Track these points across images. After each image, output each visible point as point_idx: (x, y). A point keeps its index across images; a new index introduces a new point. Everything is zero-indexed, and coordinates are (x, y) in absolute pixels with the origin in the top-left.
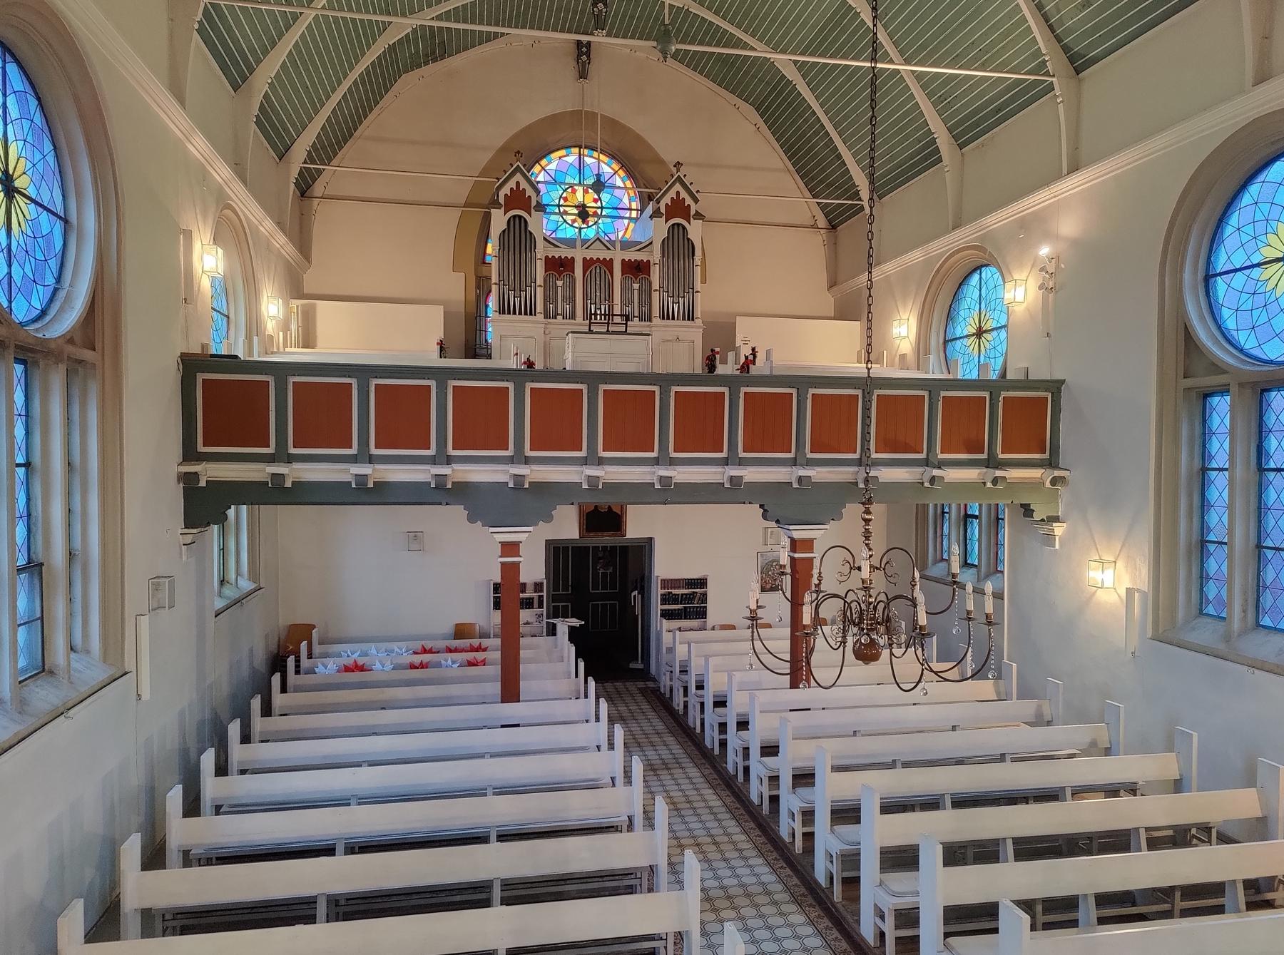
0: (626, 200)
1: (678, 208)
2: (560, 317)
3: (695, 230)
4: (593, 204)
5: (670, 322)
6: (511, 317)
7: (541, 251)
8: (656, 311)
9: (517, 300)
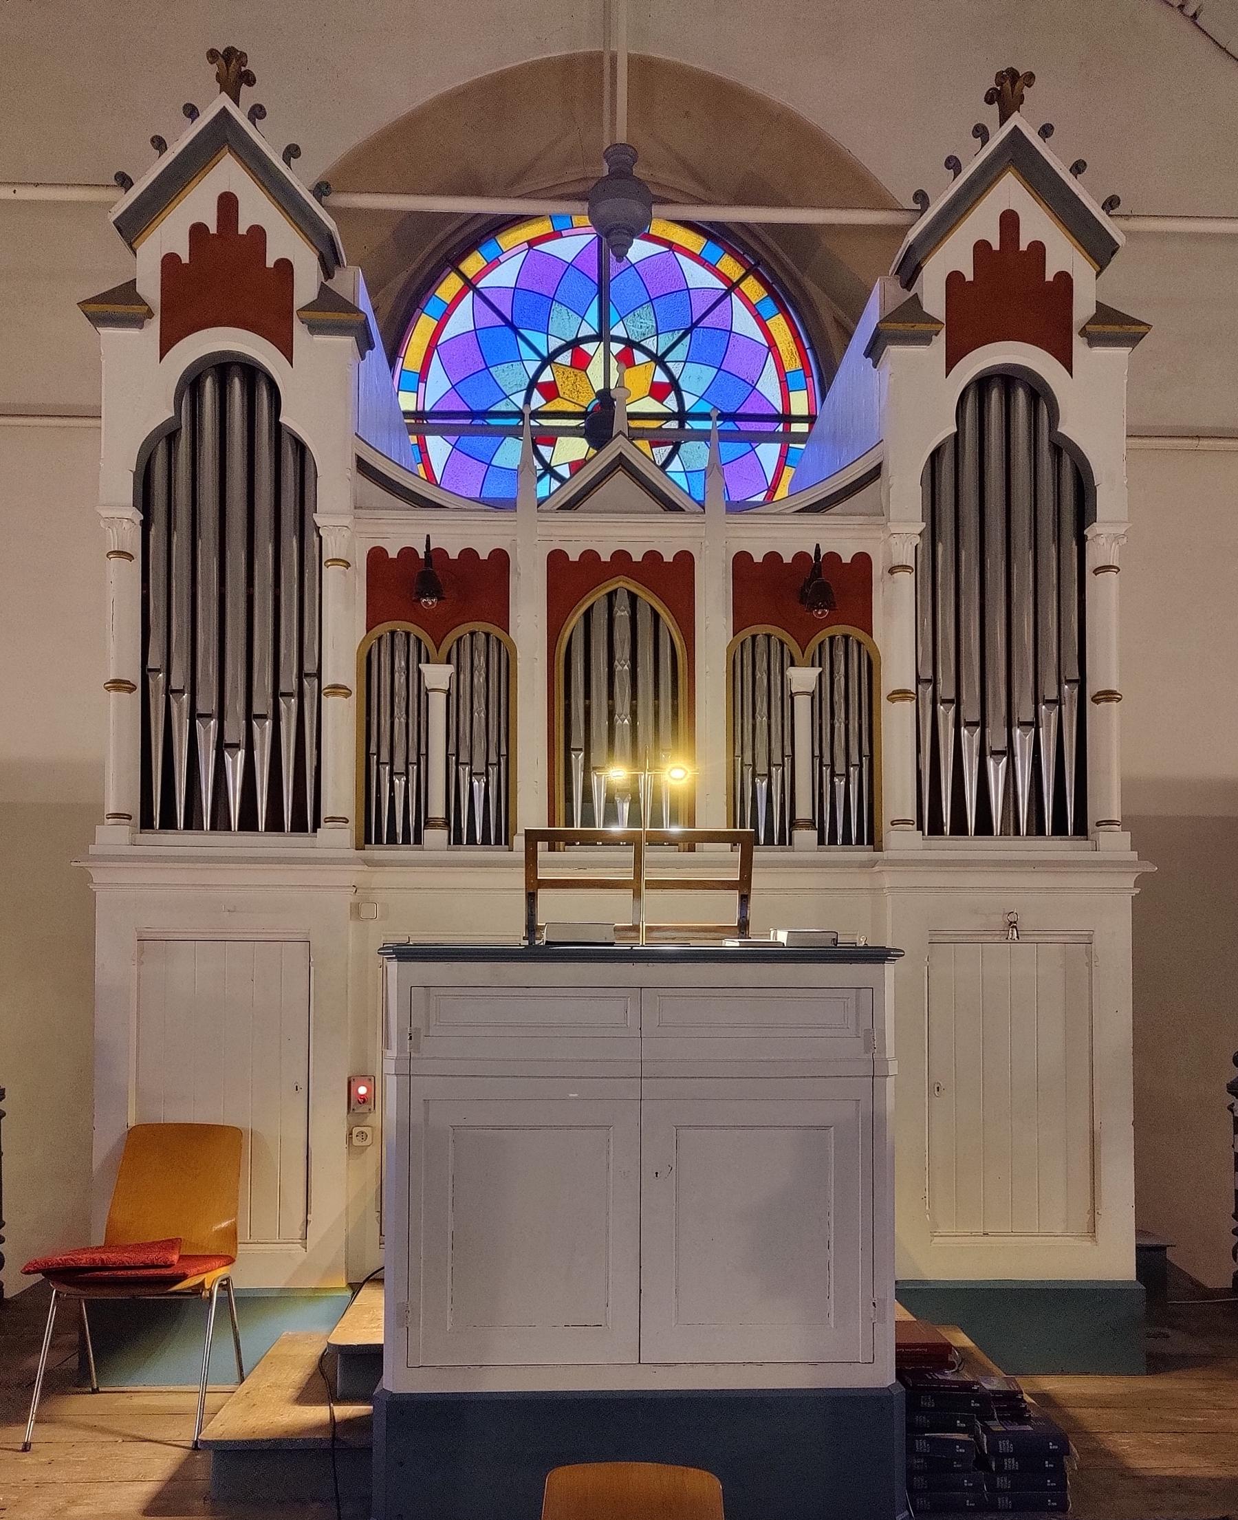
0: (769, 386)
1: (1012, 296)
2: (435, 837)
3: (1092, 398)
4: (650, 405)
5: (971, 846)
6: (205, 841)
7: (347, 528)
8: (899, 792)
9: (235, 765)
